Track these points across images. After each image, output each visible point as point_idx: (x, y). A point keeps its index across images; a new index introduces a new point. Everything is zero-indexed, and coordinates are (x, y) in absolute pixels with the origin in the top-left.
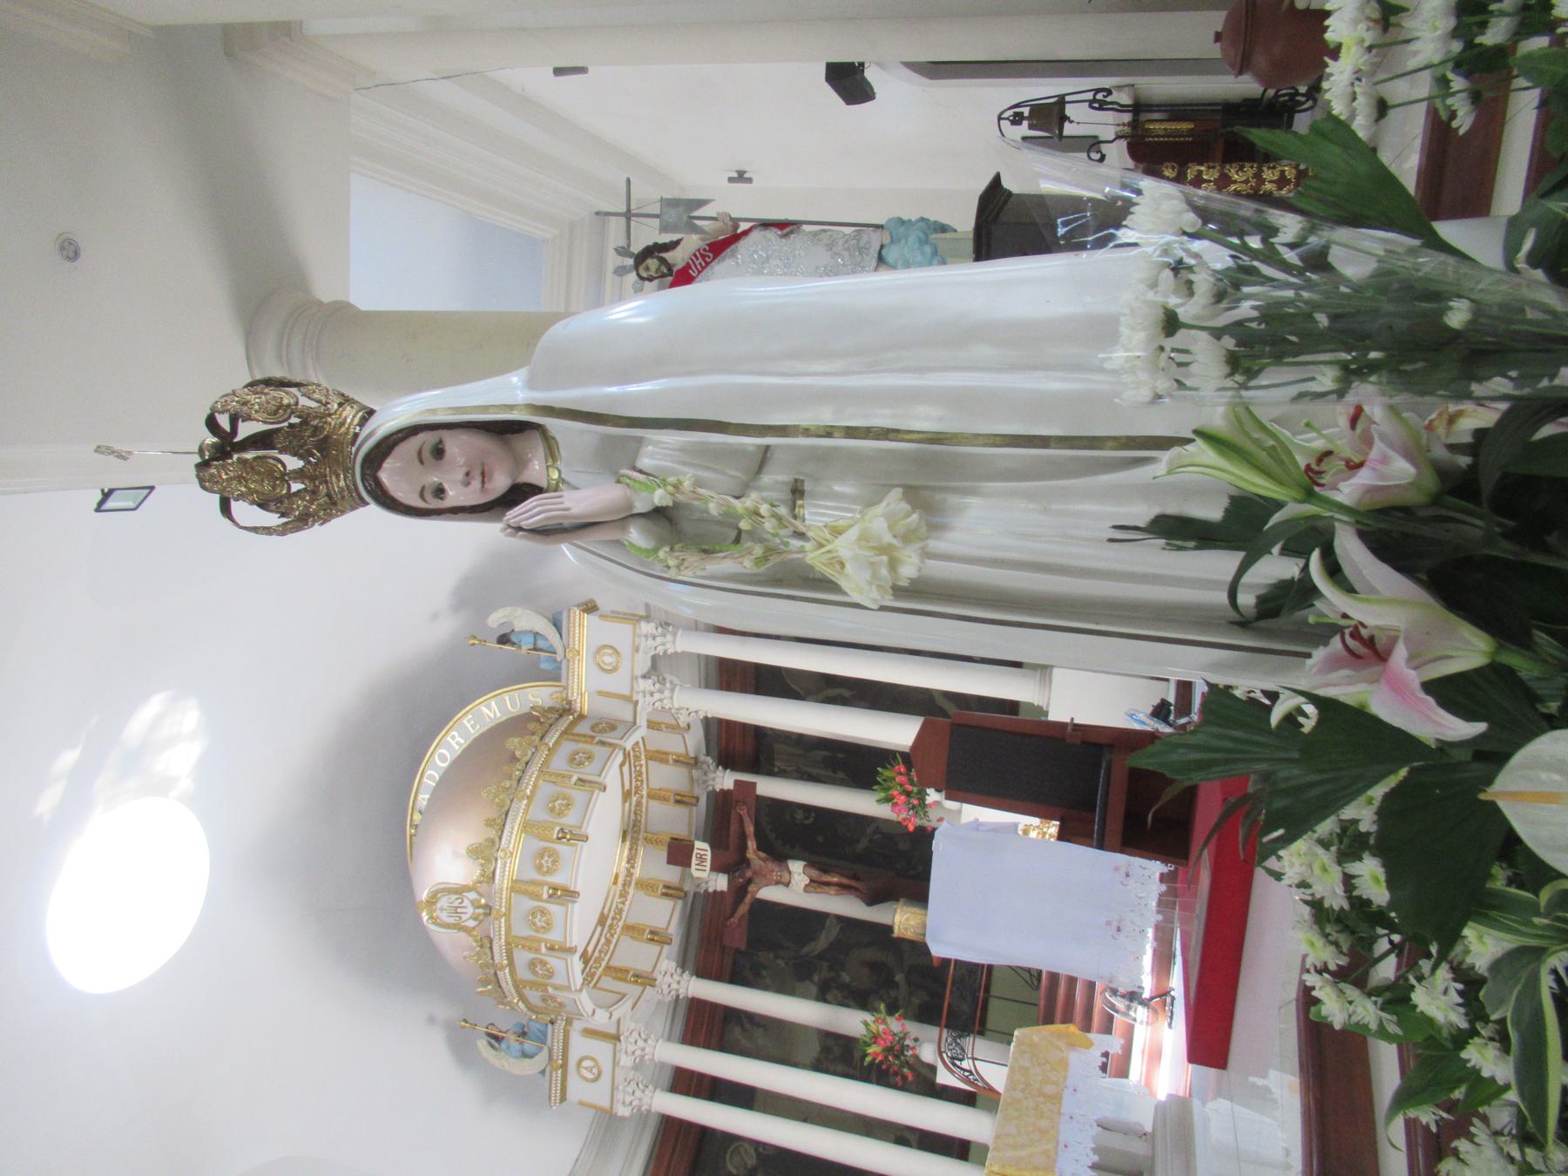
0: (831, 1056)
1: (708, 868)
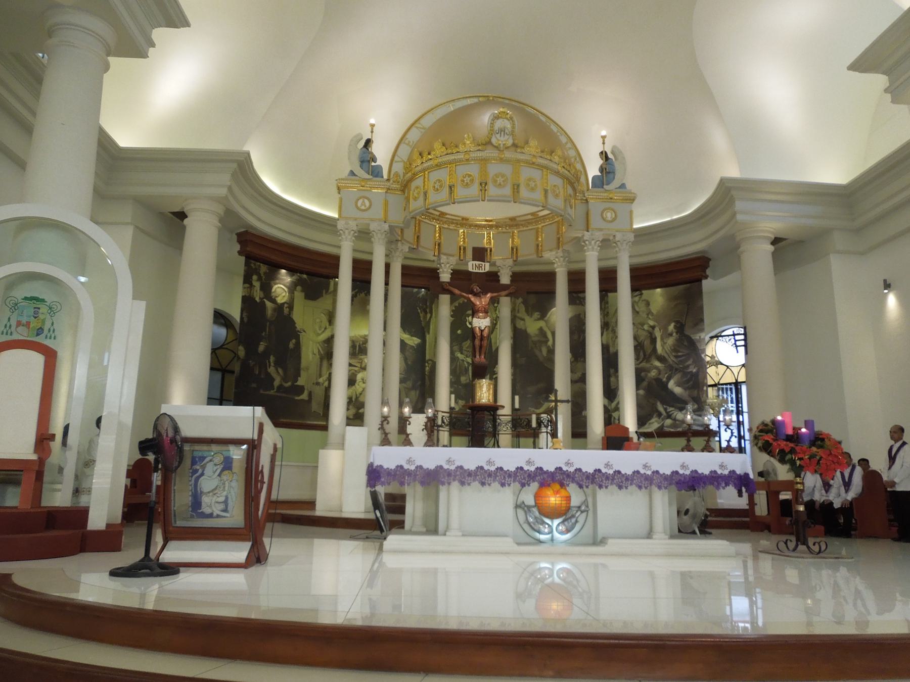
1: (474, 271)
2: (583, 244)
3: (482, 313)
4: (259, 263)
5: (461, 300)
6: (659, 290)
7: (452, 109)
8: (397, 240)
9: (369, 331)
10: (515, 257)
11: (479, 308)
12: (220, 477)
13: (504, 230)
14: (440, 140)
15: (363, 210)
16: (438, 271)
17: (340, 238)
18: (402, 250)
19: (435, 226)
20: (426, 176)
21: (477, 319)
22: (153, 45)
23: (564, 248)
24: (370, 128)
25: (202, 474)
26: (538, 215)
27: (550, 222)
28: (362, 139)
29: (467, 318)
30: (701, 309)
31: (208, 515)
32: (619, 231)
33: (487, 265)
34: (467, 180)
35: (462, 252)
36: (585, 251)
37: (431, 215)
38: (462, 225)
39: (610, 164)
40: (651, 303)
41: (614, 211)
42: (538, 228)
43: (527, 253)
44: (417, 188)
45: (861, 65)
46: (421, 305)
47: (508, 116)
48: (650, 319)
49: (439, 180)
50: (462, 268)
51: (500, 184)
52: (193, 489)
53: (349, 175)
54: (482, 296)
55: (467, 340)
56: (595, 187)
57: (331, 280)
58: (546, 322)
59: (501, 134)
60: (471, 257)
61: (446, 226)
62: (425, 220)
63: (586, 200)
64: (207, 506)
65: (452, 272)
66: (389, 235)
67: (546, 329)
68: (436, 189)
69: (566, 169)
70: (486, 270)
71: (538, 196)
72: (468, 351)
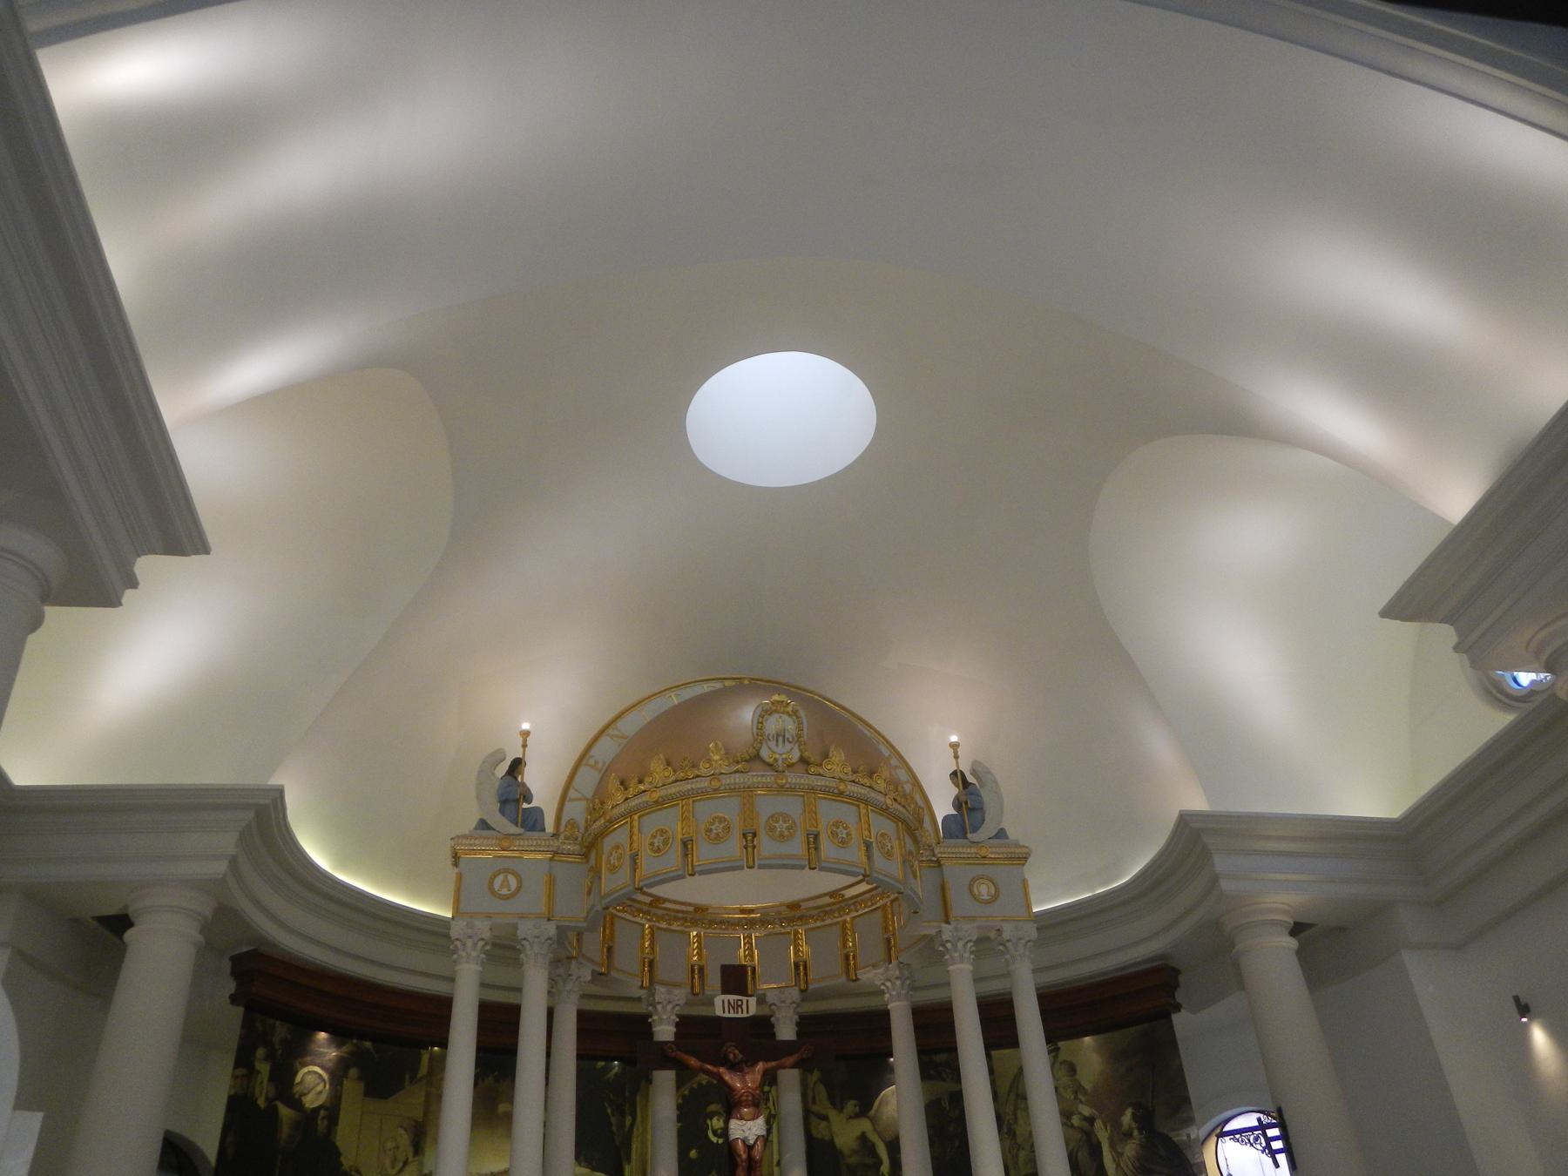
1: (726, 1015)
2: (941, 948)
4: (271, 1021)
5: (703, 1079)
6: (1087, 1039)
7: (676, 702)
8: (568, 958)
10: (802, 982)
11: (742, 1095)
13: (778, 929)
14: (661, 756)
15: (507, 897)
16: (650, 1020)
17: (455, 956)
18: (579, 977)
19: (643, 925)
20: (636, 824)
21: (738, 1122)
22: (133, 583)
23: (901, 959)
24: (521, 739)
26: (843, 896)
27: (867, 910)
28: (505, 758)
29: (709, 1122)
30: (1180, 1072)
33: (753, 1001)
34: (717, 828)
35: (696, 976)
37: (635, 905)
39: (971, 794)
40: (1078, 1069)
41: (993, 883)
42: (845, 921)
43: (826, 974)
44: (617, 847)
45: (1403, 607)
47: (790, 709)
48: (1081, 1102)
49: (662, 830)
50: (702, 1011)
51: (782, 835)
53: (476, 829)
54: (746, 1070)
56: (951, 837)
57: (423, 1052)
58: (874, 1121)
59: (777, 741)
60: (719, 989)
61: (663, 925)
62: (620, 914)
63: (938, 861)
65: (678, 1020)
66: (555, 946)
67: (874, 1138)
68: (655, 848)
69: (900, 804)
70: (751, 1014)
71: (855, 854)
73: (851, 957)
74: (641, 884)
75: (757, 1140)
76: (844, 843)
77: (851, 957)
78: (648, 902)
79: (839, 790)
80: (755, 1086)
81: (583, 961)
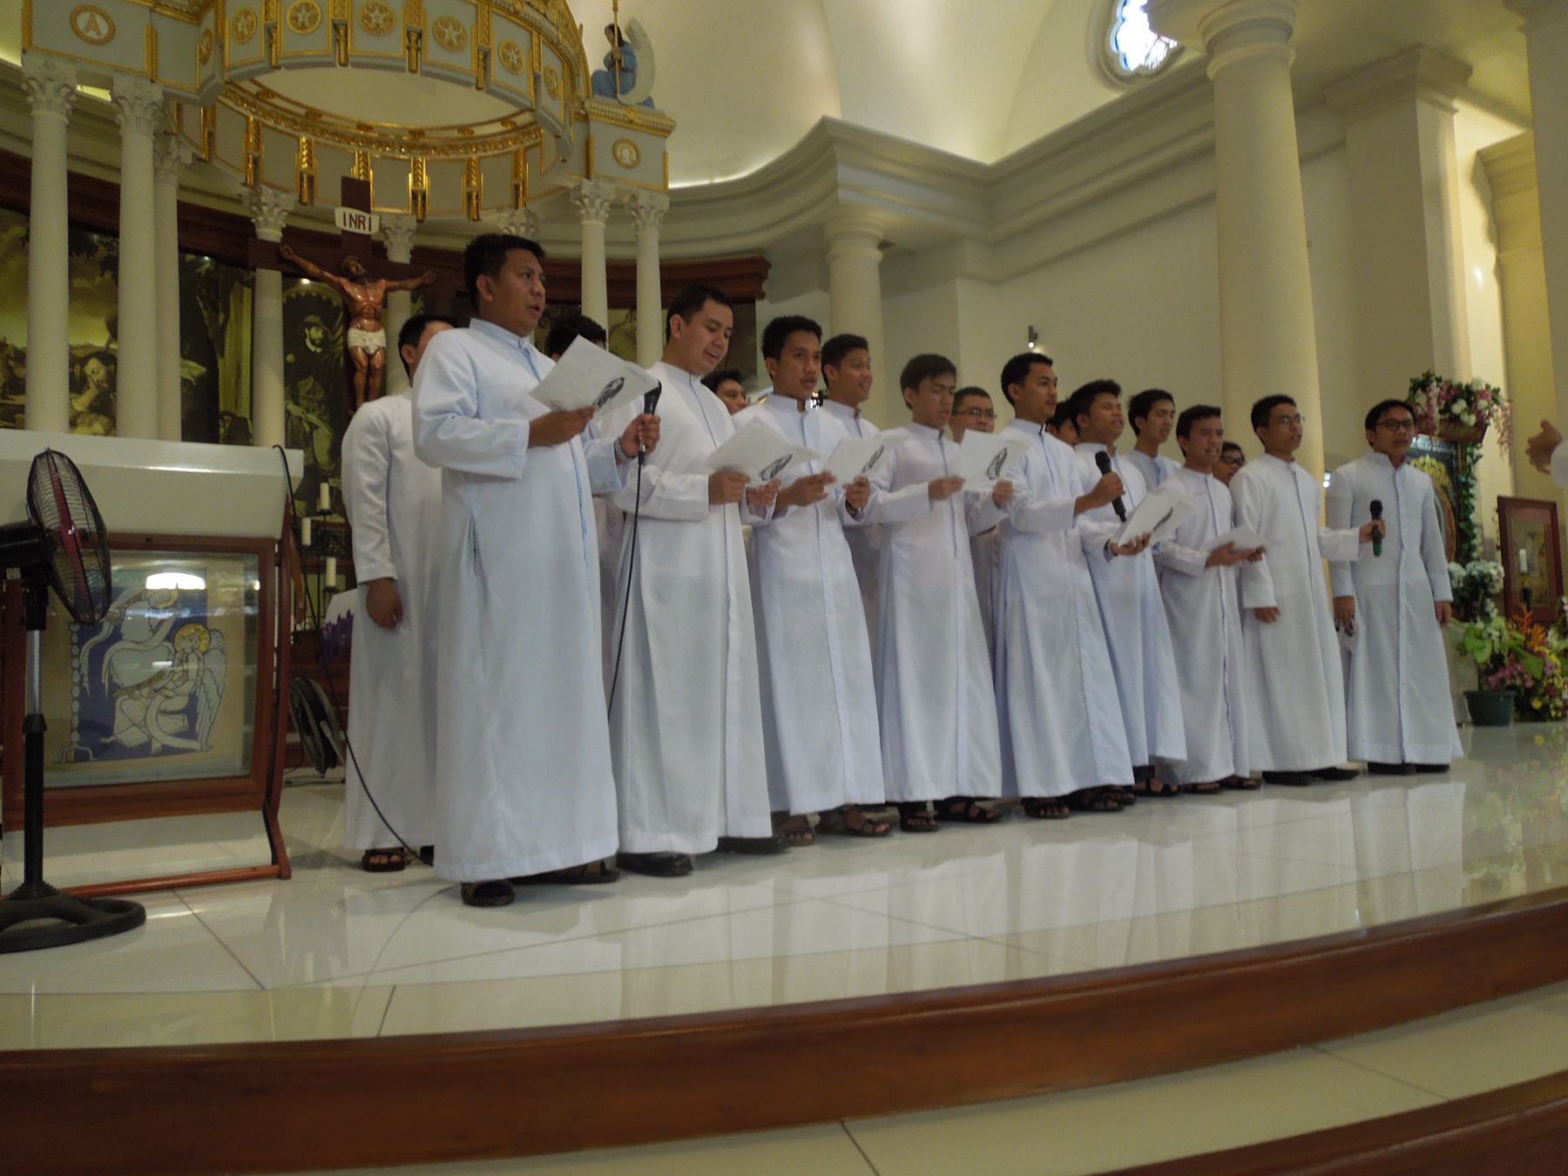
0: (11, 363)
1: (347, 228)
2: (578, 203)
3: (366, 319)
8: (165, 133)
9: (113, 328)
10: (419, 212)
11: (364, 307)
12: (173, 642)
18: (179, 158)
19: (248, 118)
25: (116, 637)
26: (473, 132)
27: (495, 152)
29: (307, 331)
31: (132, 749)
32: (644, 188)
35: (305, 185)
36: (577, 220)
37: (237, 91)
38: (304, 129)
41: (635, 148)
42: (470, 160)
43: (447, 209)
44: (247, 13)
46: (204, 291)
49: (307, 5)
52: (86, 679)
55: (306, 377)
60: (338, 197)
61: (271, 123)
64: (134, 725)
68: (299, 24)
71: (522, 84)
72: (311, 400)
73: (474, 197)
74: (280, 62)
75: (377, 350)
76: (514, 69)
77: (474, 197)
78: (254, 92)
79: (514, 9)
80: (377, 302)
81: (185, 142)
